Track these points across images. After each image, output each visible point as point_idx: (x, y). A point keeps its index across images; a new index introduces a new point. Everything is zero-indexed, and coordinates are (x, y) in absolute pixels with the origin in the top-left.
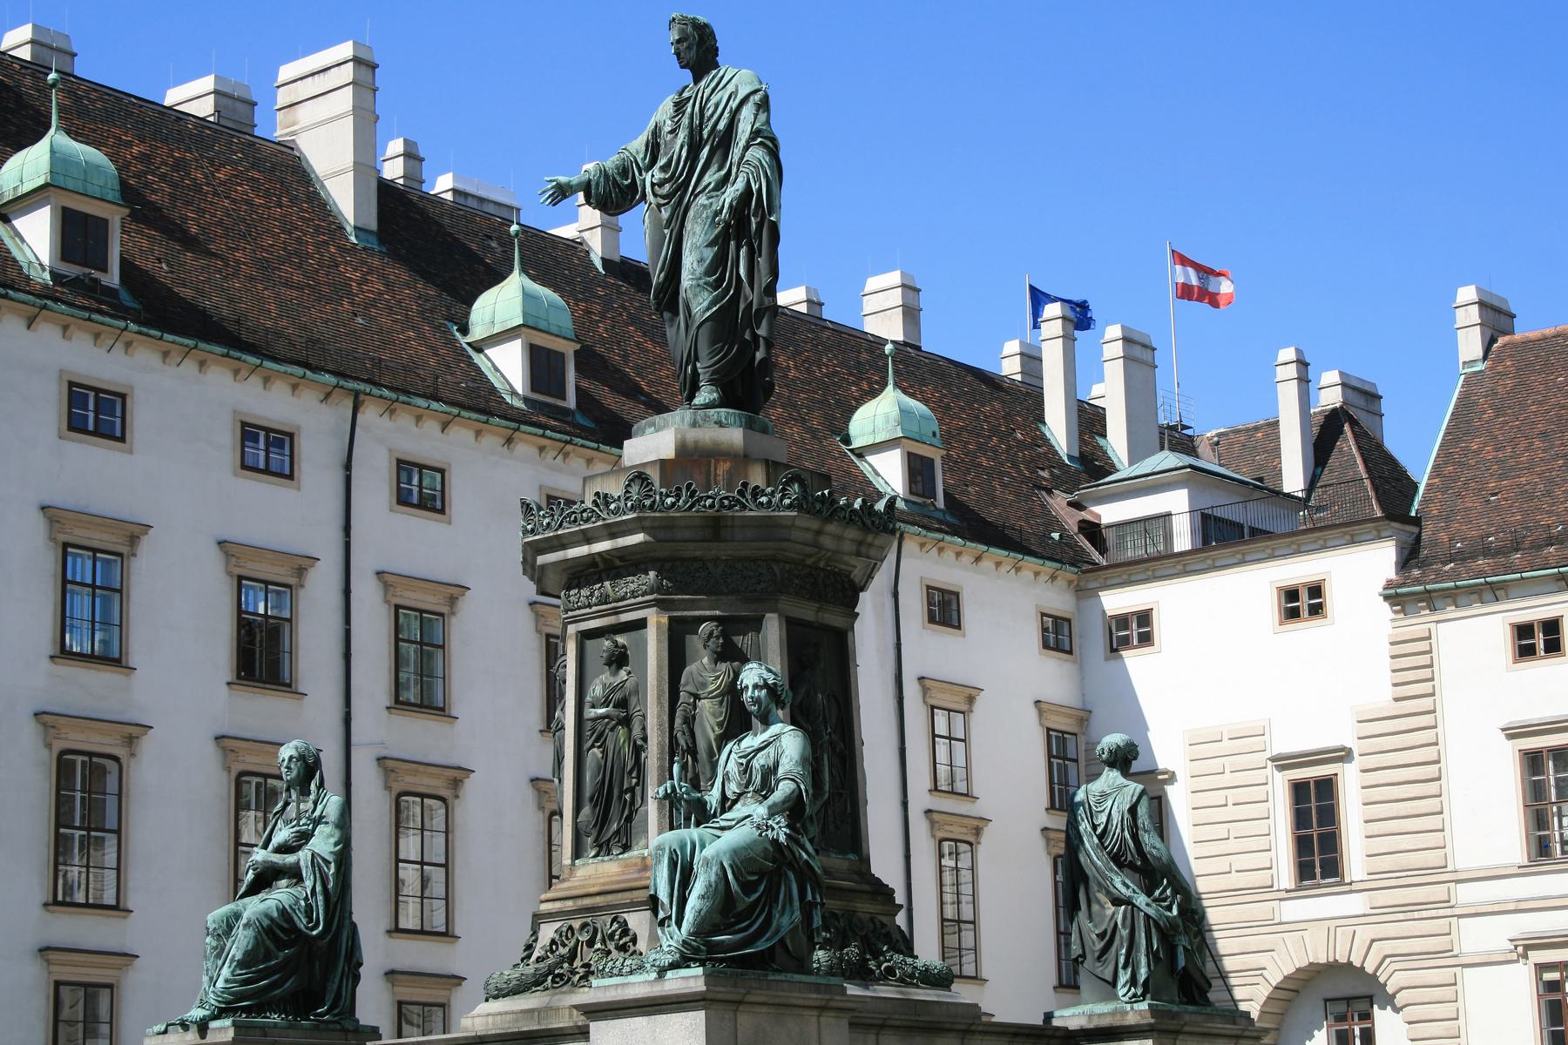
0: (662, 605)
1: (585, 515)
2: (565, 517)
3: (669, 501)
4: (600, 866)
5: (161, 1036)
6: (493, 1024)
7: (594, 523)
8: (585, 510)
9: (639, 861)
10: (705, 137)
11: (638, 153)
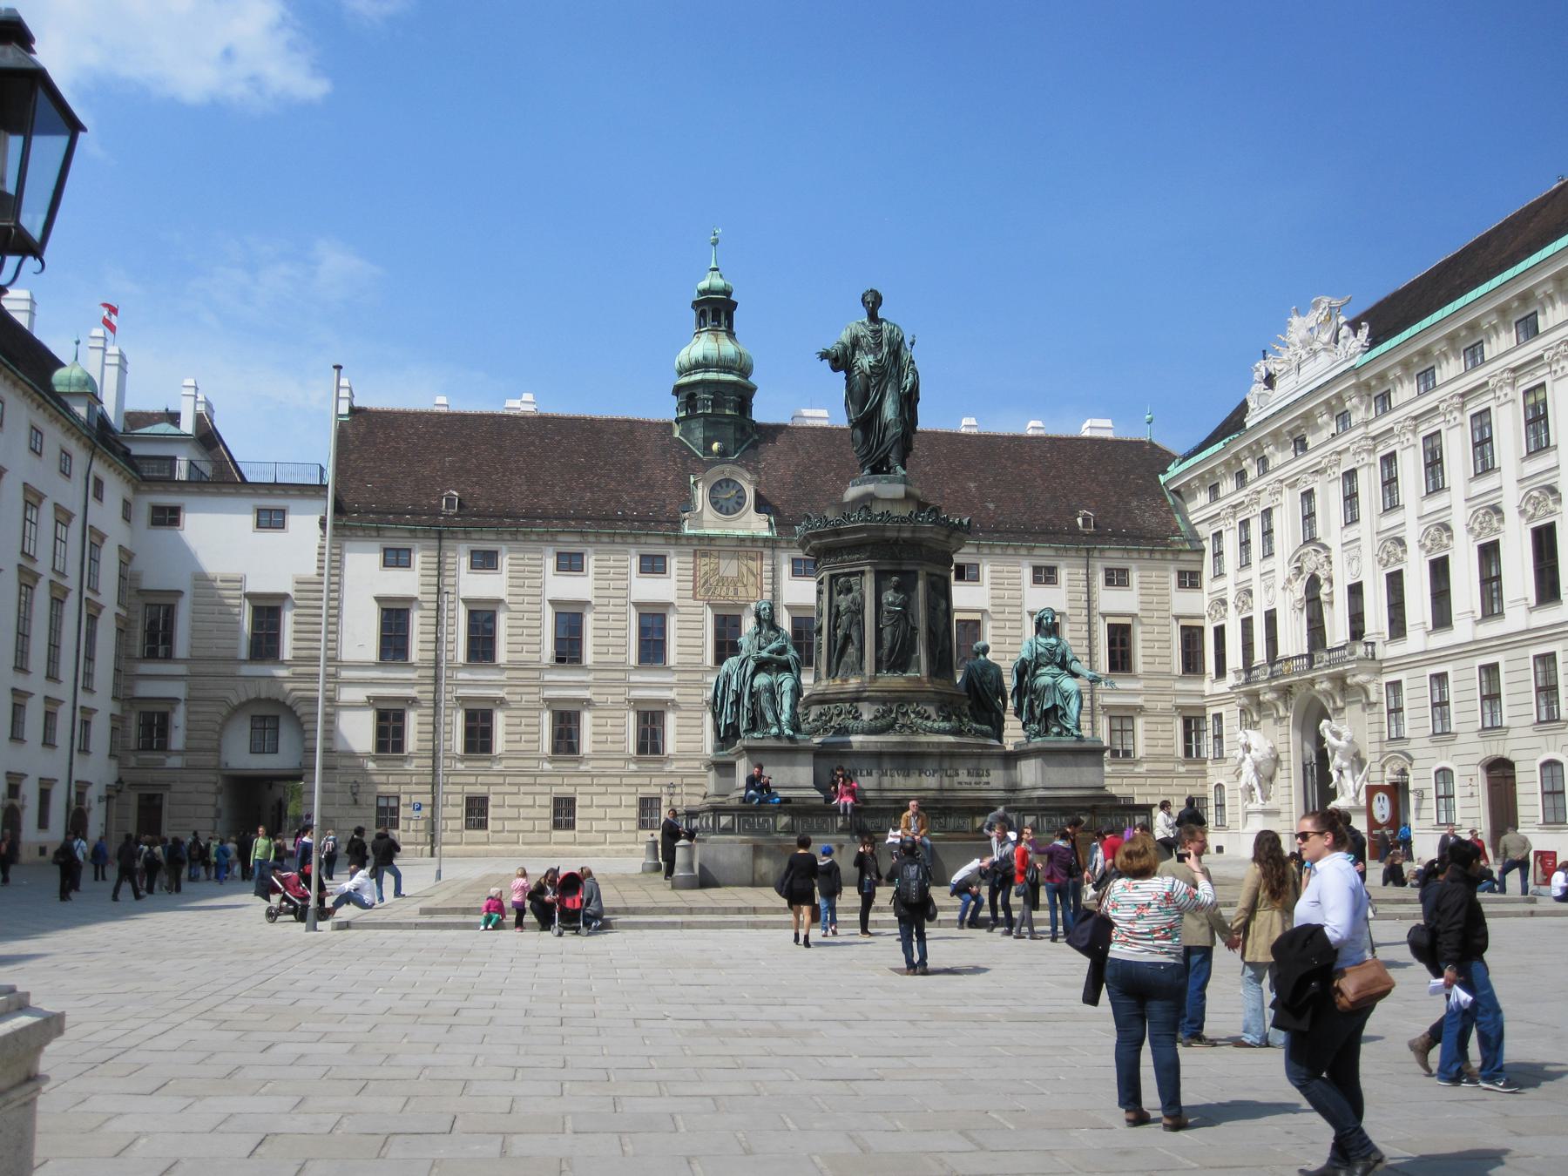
4: (893, 680)
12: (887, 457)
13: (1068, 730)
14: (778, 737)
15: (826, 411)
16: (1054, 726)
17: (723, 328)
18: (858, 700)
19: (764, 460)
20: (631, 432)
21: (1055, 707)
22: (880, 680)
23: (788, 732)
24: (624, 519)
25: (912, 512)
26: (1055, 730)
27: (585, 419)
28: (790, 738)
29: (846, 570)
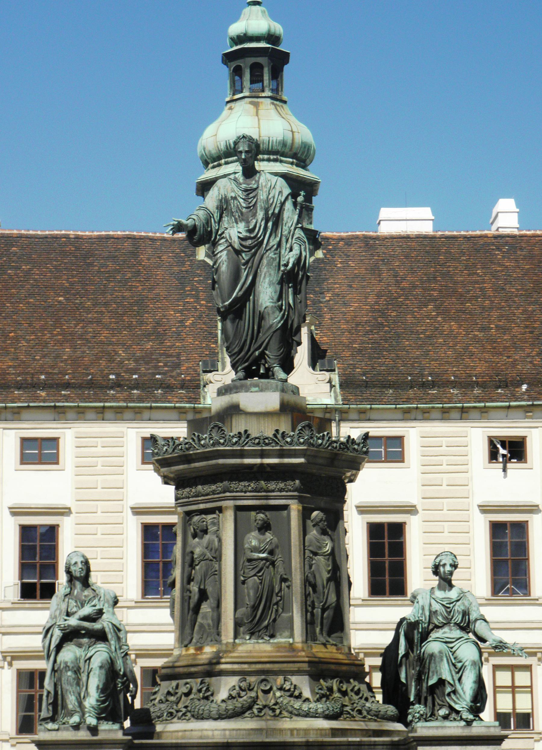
0: (301, 500)
1: (267, 441)
2: (251, 440)
3: (320, 441)
4: (257, 647)
5: (54, 732)
6: (230, 735)
7: (273, 447)
8: (267, 438)
9: (287, 645)
10: (270, 216)
11: (214, 212)
12: (262, 355)
13: (458, 712)
14: (77, 727)
15: (426, 212)
16: (441, 707)
17: (268, 93)
18: (210, 674)
19: (328, 290)
20: (135, 254)
21: (441, 682)
22: (240, 648)
23: (91, 721)
24: (117, 385)
25: (277, 431)
26: (443, 712)
27: (67, 237)
28: (94, 730)
29: (202, 506)
